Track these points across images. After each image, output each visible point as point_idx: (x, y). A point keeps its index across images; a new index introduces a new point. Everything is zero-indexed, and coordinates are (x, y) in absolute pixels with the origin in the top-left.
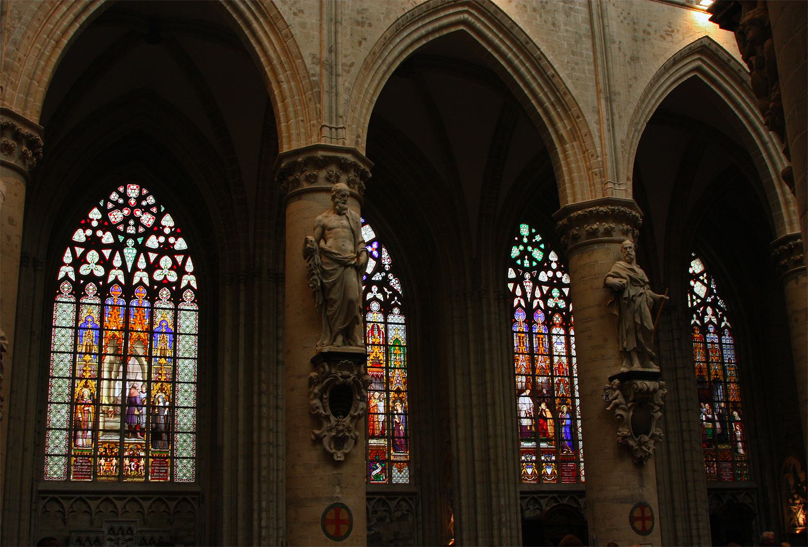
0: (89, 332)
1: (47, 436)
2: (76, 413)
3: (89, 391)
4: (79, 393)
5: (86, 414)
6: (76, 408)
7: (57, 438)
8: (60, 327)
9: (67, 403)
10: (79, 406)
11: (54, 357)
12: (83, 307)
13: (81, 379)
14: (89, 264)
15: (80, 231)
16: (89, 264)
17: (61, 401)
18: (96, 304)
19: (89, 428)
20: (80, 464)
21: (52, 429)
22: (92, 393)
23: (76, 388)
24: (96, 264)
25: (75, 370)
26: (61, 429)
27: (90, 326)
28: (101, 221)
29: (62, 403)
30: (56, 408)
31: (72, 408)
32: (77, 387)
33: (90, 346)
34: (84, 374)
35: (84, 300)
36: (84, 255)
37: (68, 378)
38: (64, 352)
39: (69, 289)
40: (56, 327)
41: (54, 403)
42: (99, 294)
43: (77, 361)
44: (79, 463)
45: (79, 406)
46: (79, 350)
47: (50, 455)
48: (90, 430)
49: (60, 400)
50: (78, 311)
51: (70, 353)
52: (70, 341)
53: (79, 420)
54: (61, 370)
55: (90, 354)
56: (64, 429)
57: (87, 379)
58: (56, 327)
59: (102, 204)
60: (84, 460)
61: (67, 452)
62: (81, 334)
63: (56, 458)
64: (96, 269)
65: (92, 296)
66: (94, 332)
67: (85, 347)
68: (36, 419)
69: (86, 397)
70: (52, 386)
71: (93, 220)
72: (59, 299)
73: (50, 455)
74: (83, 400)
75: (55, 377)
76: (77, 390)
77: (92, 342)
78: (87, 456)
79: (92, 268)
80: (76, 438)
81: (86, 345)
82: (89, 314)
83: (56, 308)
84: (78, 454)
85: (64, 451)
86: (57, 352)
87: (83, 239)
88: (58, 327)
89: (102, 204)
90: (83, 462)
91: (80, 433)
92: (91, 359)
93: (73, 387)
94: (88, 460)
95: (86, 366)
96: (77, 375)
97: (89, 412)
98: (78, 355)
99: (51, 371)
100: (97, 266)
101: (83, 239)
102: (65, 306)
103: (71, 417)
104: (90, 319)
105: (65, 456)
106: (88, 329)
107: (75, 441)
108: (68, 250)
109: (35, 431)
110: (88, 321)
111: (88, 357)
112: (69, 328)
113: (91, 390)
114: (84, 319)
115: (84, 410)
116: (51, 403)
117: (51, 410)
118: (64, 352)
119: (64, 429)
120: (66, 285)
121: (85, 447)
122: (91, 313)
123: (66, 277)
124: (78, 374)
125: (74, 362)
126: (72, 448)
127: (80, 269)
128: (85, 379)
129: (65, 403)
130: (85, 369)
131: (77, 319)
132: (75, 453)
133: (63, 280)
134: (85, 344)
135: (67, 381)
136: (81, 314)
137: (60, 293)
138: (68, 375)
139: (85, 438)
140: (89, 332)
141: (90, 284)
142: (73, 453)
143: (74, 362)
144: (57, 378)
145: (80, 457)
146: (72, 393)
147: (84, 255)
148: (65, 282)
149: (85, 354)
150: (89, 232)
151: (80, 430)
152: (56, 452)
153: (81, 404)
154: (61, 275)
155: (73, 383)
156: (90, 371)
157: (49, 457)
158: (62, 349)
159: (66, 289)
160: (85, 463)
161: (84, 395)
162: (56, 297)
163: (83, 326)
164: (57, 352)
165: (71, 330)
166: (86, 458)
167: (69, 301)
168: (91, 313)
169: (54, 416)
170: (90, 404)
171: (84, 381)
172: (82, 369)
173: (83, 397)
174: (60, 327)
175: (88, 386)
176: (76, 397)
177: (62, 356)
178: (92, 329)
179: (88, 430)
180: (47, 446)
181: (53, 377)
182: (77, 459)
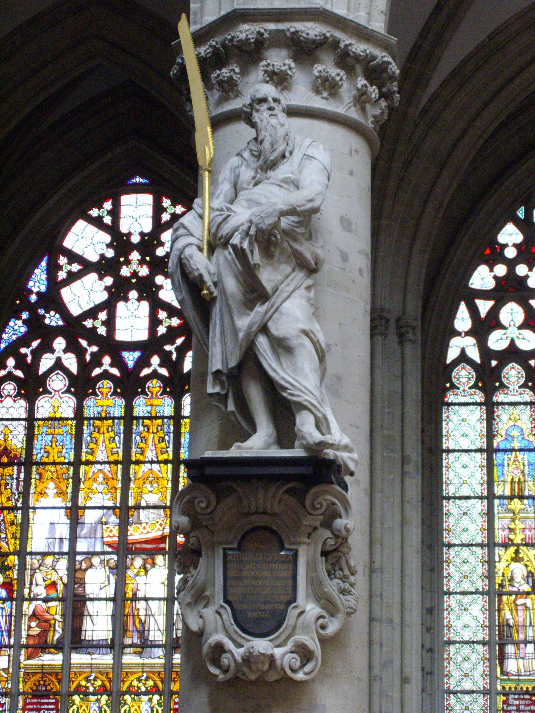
0: (516, 457)
1: (445, 656)
2: (499, 610)
3: (524, 568)
4: (503, 574)
5: (520, 613)
6: (500, 601)
7: (466, 659)
8: (458, 451)
9: (482, 593)
10: (505, 598)
11: (449, 506)
12: (499, 411)
13: (505, 545)
14: (504, 328)
15: (482, 271)
16: (504, 328)
17: (470, 590)
18: (525, 404)
19: (530, 639)
20: (515, 708)
21: (454, 642)
22: (530, 572)
23: (497, 564)
24: (520, 327)
25: (493, 529)
26: (473, 642)
27: (516, 445)
28: (523, 248)
29: (472, 593)
30: (460, 604)
31: (491, 603)
32: (499, 562)
33: (519, 482)
34: (512, 536)
35: (500, 397)
36: (494, 313)
37: (481, 545)
38: (469, 498)
39: (469, 379)
40: (449, 451)
41: (456, 593)
42: (530, 384)
43: (496, 511)
44: (513, 705)
45: (505, 598)
46: (498, 491)
47: (455, 693)
48: (530, 642)
49: (466, 586)
50: (490, 418)
51: (481, 498)
52: (480, 475)
53: (508, 625)
54: (465, 530)
55: (521, 497)
56: (478, 642)
57: (518, 545)
58: (449, 451)
59: (521, 213)
60: (523, 699)
61: (488, 687)
62: (500, 461)
63: (467, 698)
64: (521, 337)
65: (516, 388)
66: (526, 456)
67: (509, 485)
68: (422, 624)
69: (517, 580)
70: (448, 562)
71: (506, 246)
72: (451, 398)
73: (455, 693)
74: (513, 586)
75: (454, 545)
76: (500, 567)
77: (524, 476)
78: (527, 692)
79: (511, 336)
80: (502, 657)
81: (512, 482)
82: (513, 423)
83: (448, 417)
84: (510, 688)
85: (481, 683)
86: (455, 498)
87: (490, 284)
88: (454, 451)
89: (521, 213)
90: (520, 705)
91: (510, 649)
92: (523, 507)
93: (491, 563)
94: (530, 699)
95: (513, 520)
96: (498, 539)
97: (526, 608)
98: (496, 502)
99: (445, 534)
100: (521, 331)
101: (490, 284)
102: (464, 411)
103: (491, 618)
104: (515, 433)
105: (484, 692)
106: (512, 450)
107: (502, 664)
108: (463, 307)
109: (423, 646)
110: (513, 437)
111: (516, 504)
112: (476, 451)
113: (526, 566)
114: (503, 433)
115: (516, 605)
116: (450, 593)
117: (449, 606)
118: (469, 498)
119: (478, 642)
120: (463, 373)
121: (525, 675)
122: (516, 420)
123: (463, 357)
124: (500, 536)
125: (490, 515)
126: (497, 678)
127: (487, 340)
128: (513, 545)
129: (476, 592)
130: (512, 526)
131: (490, 435)
132: (504, 688)
133: (456, 362)
134: (509, 480)
135: (478, 551)
136: (497, 424)
137: (453, 387)
138: (479, 540)
139: (523, 658)
140: (516, 457)
141: (510, 366)
142: (499, 688)
143: (490, 515)
144: (459, 545)
145: (514, 694)
146: (490, 575)
147: (494, 313)
148: (459, 367)
149: (511, 498)
150: (501, 270)
151: (511, 643)
152: (467, 685)
153: (510, 594)
154: (452, 354)
155: (491, 554)
156: (524, 530)
157: (451, 695)
158: (465, 491)
159: (464, 380)
160: (526, 705)
161: (515, 576)
162: (445, 396)
163: (502, 446)
164: (455, 498)
165: (479, 454)
166: (527, 697)
167: (471, 401)
168: (516, 420)
169: (458, 617)
170: (528, 593)
171: (513, 549)
172: (506, 526)
173: (511, 579)
174: (458, 451)
175: (522, 559)
176: (498, 580)
177: (464, 504)
178: (521, 450)
179: (526, 642)
180: (447, 675)
181: (450, 546)
182: (508, 699)
